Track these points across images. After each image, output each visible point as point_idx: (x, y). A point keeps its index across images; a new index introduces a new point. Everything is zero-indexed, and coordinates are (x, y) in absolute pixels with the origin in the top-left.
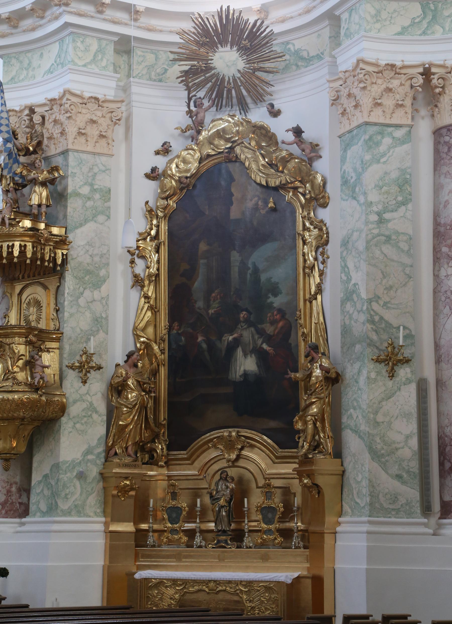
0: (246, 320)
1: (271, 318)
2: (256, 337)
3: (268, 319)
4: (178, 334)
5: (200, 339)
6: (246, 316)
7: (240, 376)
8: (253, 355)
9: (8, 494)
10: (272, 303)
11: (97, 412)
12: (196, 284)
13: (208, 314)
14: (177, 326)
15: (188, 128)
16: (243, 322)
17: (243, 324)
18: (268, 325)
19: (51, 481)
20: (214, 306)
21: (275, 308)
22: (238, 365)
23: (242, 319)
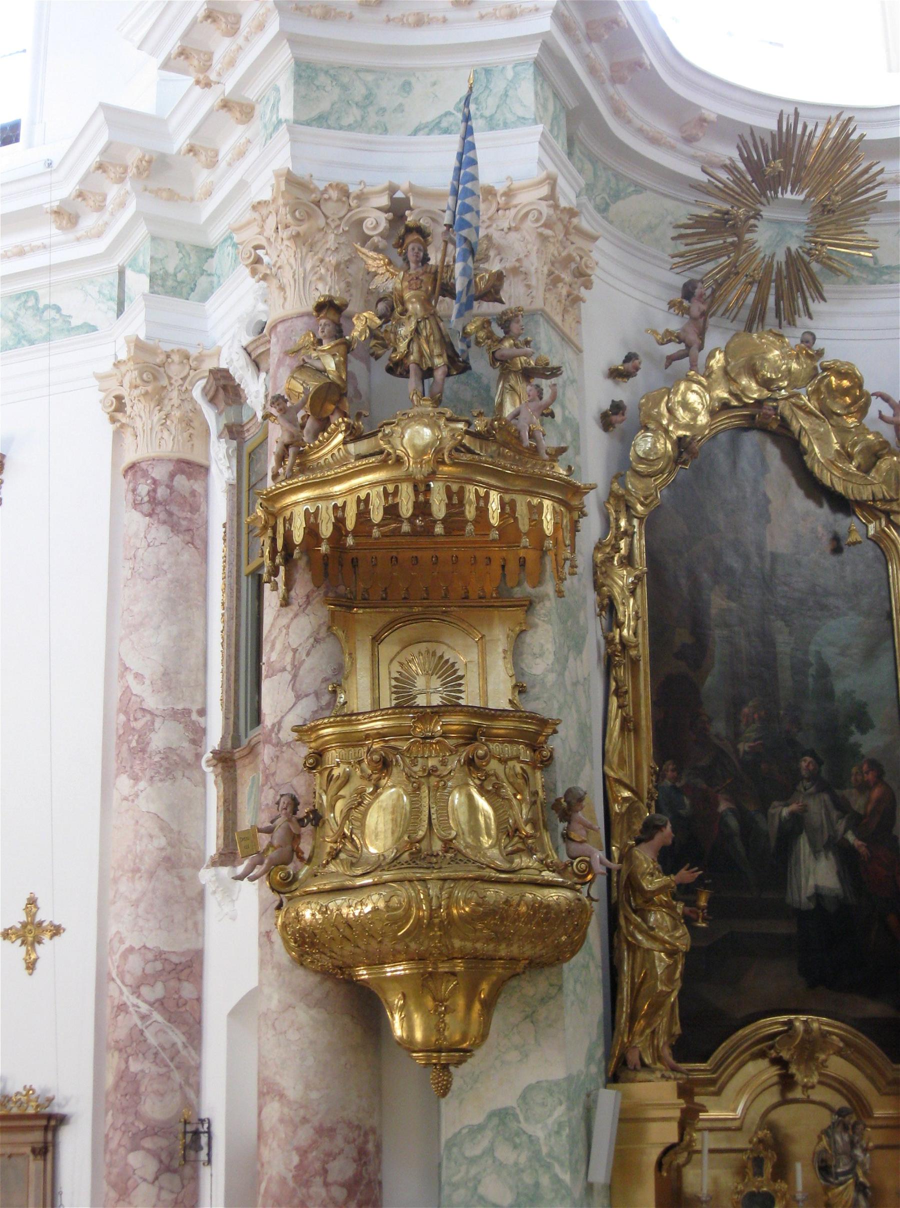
0: (814, 777)
1: (859, 778)
2: (835, 814)
3: (853, 778)
4: (674, 787)
5: (723, 806)
6: (811, 767)
7: (809, 898)
8: (831, 855)
9: (360, 1159)
10: (857, 745)
11: (593, 958)
12: (710, 681)
13: (737, 751)
14: (673, 771)
15: (668, 337)
16: (808, 779)
17: (808, 784)
18: (854, 791)
19: (524, 1125)
20: (748, 735)
21: (863, 756)
22: (803, 872)
23: (804, 773)
